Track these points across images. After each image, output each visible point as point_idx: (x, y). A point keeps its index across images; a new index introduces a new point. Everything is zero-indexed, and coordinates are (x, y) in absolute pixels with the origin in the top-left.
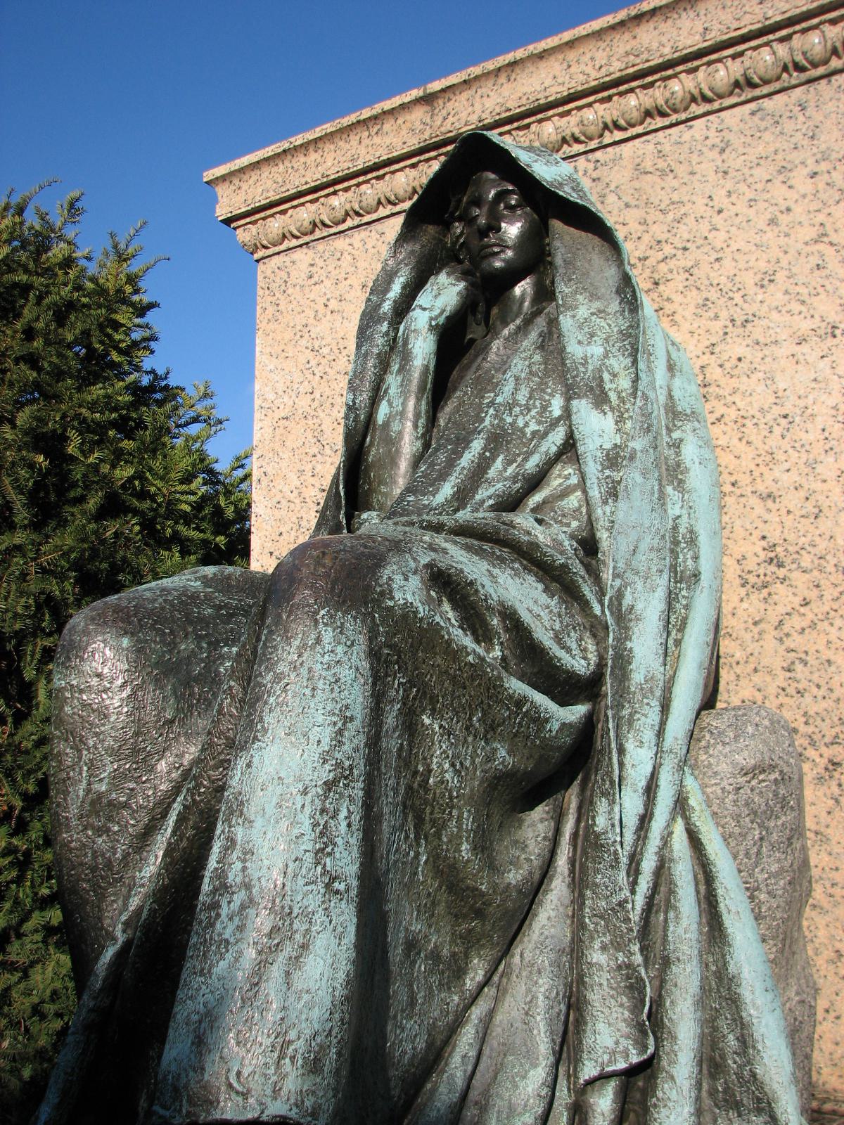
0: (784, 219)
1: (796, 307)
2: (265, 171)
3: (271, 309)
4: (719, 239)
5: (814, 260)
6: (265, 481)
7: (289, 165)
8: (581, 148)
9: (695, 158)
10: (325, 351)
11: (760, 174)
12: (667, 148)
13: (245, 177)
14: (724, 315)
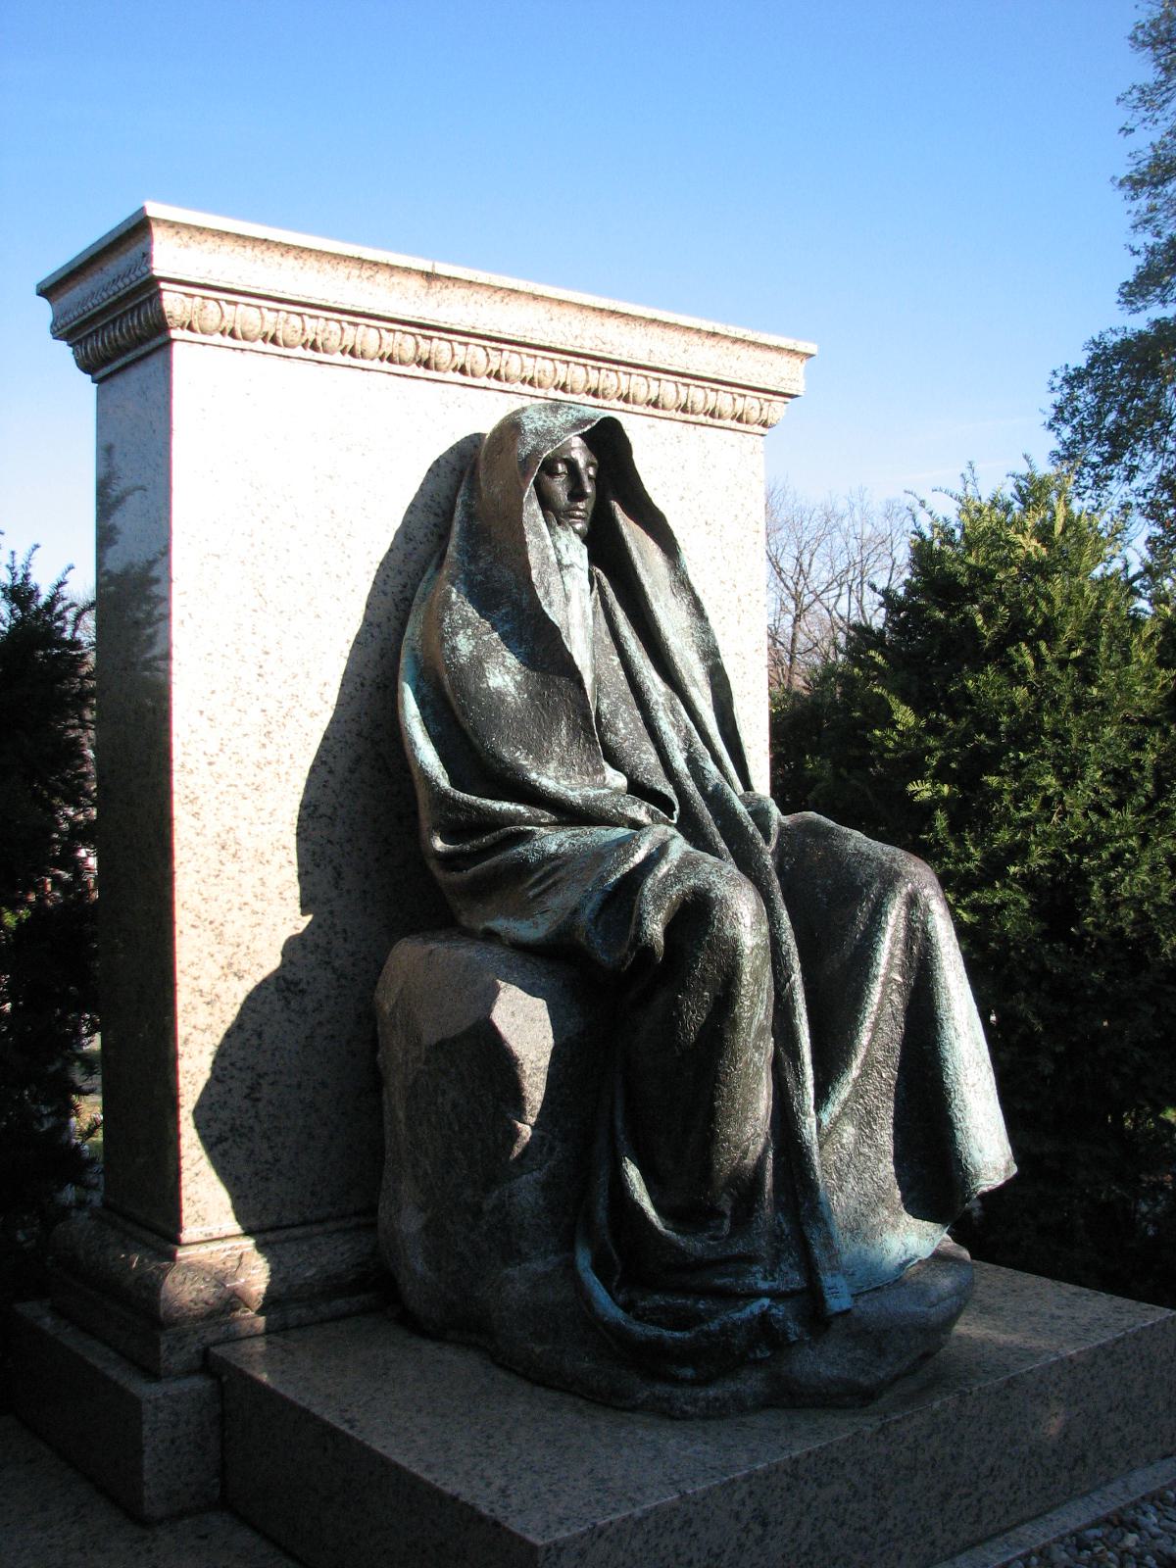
7: (259, 255)
13: (199, 237)
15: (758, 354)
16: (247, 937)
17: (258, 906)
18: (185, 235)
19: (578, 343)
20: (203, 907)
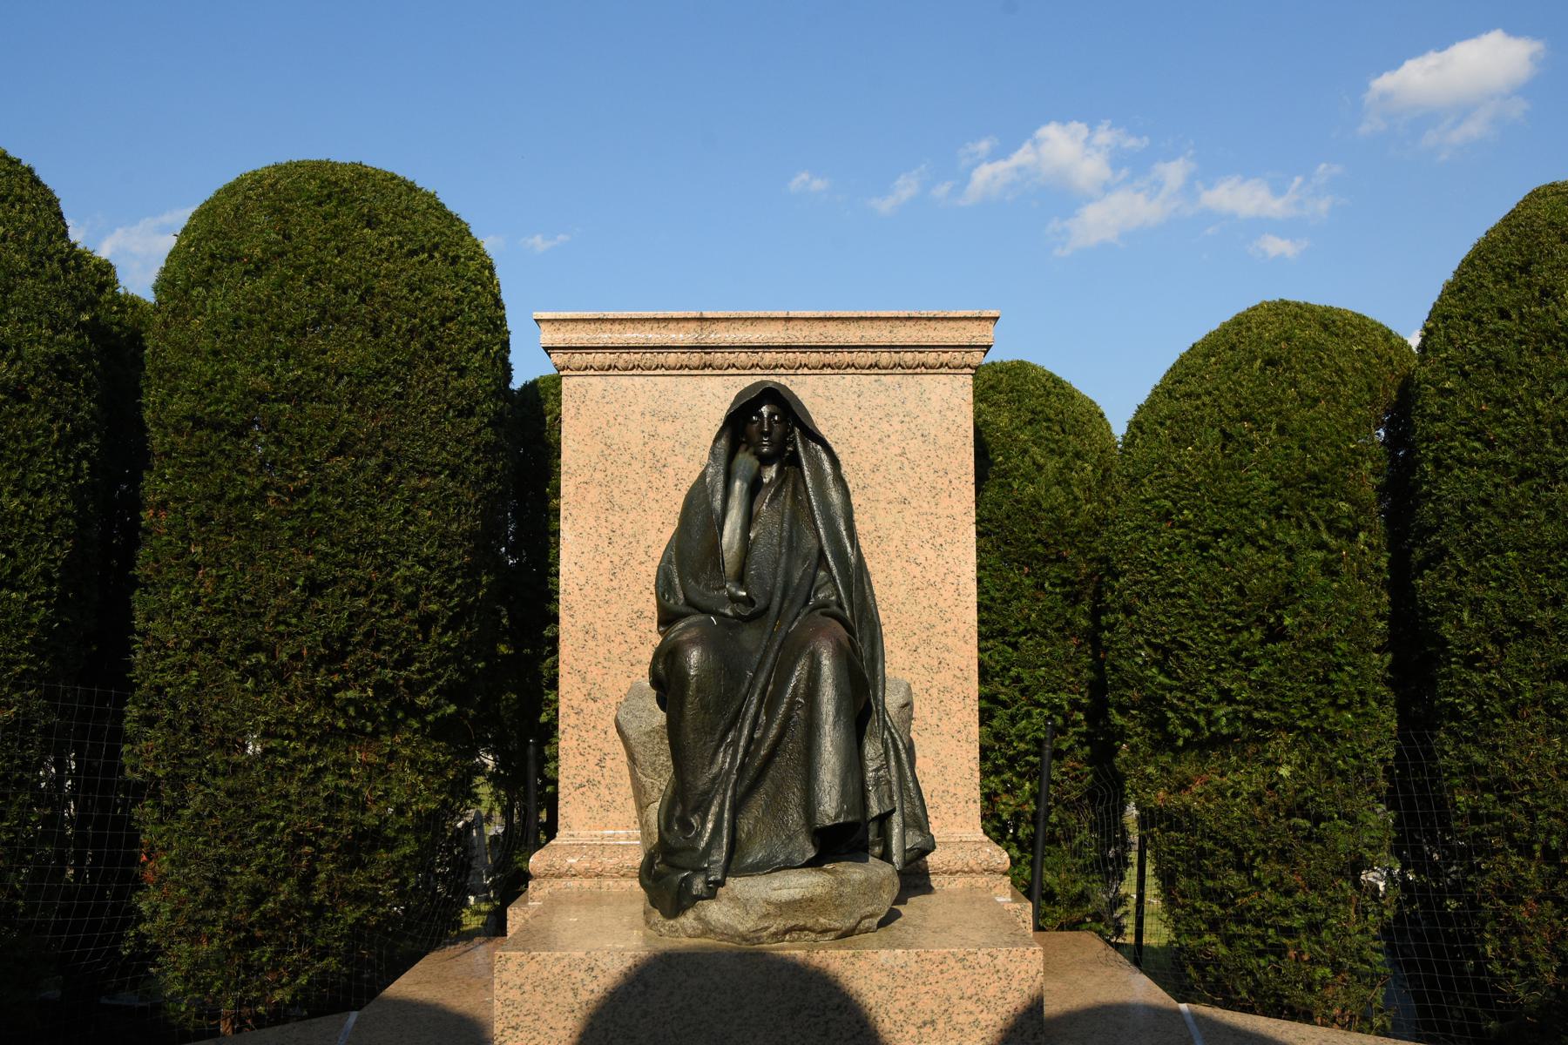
2: (580, 326)
3: (573, 411)
4: (854, 442)
6: (570, 519)
15: (951, 324)
16: (599, 680)
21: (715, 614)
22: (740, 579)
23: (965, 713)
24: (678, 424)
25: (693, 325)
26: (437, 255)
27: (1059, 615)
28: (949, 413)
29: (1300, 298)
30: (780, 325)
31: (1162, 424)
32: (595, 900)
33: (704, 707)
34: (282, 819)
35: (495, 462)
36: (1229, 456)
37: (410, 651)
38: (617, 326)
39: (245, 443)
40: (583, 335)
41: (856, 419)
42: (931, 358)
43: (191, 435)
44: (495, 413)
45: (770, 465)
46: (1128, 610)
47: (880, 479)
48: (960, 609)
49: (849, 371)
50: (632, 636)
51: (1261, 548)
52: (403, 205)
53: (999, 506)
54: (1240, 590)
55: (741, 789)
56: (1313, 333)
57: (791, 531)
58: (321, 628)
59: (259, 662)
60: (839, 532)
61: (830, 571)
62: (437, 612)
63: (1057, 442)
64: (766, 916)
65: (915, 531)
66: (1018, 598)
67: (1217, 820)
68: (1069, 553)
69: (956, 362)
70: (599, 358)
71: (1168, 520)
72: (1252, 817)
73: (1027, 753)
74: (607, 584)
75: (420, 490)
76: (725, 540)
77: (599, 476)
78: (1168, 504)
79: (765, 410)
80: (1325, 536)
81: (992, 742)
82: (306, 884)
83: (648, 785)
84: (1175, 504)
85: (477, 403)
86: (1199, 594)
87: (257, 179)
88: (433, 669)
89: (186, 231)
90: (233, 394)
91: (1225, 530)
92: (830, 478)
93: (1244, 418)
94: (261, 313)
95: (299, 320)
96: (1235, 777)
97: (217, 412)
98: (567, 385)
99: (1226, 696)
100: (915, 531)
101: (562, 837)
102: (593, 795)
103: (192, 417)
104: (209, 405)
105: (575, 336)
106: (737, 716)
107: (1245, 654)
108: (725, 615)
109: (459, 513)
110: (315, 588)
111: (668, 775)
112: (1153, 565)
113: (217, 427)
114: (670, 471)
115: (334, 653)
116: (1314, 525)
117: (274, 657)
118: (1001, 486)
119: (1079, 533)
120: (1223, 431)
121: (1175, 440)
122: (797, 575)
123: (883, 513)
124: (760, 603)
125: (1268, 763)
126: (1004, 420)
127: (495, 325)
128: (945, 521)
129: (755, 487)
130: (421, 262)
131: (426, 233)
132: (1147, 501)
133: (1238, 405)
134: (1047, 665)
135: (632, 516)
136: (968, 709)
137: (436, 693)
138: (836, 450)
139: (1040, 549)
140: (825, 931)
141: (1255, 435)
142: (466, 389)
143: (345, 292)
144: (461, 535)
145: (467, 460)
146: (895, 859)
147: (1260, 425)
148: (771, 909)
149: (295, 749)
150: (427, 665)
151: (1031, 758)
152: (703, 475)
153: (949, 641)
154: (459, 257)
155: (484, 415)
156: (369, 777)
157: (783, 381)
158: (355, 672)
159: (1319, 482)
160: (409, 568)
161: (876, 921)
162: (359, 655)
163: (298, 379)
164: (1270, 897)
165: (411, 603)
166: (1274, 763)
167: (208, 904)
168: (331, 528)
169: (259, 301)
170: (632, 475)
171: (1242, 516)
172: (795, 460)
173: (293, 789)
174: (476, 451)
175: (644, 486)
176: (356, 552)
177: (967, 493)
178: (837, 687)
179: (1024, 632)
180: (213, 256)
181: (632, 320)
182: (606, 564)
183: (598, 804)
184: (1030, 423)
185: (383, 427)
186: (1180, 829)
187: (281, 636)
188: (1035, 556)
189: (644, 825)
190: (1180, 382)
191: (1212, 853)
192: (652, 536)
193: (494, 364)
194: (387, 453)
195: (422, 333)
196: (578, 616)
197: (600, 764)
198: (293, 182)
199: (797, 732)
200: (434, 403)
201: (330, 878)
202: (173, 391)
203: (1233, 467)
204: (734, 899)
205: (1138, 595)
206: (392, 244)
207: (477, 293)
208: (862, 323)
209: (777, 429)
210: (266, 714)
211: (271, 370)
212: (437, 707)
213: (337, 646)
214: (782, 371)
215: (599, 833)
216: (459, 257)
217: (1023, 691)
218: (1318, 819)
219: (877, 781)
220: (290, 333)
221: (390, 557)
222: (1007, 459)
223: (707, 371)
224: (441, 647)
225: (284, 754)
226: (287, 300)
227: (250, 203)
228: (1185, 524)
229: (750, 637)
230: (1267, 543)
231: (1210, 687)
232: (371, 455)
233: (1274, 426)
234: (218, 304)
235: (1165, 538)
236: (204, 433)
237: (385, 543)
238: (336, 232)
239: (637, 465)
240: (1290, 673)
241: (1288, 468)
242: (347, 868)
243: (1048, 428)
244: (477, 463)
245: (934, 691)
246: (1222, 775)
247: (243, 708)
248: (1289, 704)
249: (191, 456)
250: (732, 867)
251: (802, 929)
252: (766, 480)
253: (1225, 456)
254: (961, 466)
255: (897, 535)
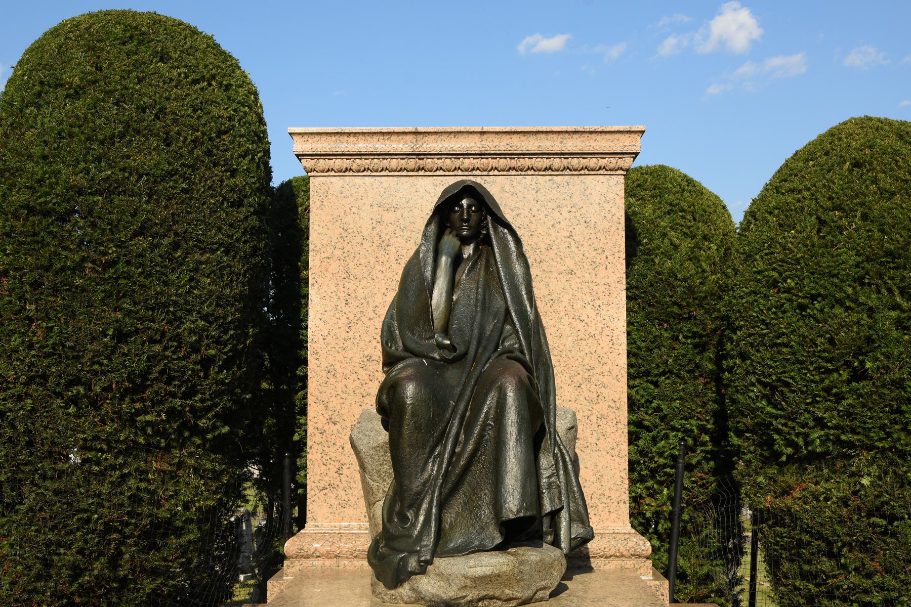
0: (558, 226)
1: (559, 260)
2: (324, 138)
3: (318, 203)
4: (533, 227)
5: (567, 244)
6: (316, 285)
8: (480, 173)
9: (526, 191)
10: (350, 231)
11: (551, 205)
12: (515, 184)
14: (532, 257)
15: (608, 136)
16: (338, 407)
17: (343, 396)
18: (306, 137)
19: (497, 148)
20: (319, 395)
21: (427, 357)
22: (446, 331)
23: (618, 435)
24: (398, 213)
25: (410, 138)
26: (214, 83)
27: (690, 360)
28: (605, 205)
29: (882, 116)
30: (476, 138)
31: (771, 213)
32: (334, 576)
33: (418, 428)
34: (96, 512)
35: (259, 242)
36: (823, 237)
37: (195, 385)
38: (351, 139)
39: (68, 226)
40: (326, 145)
41: (534, 209)
42: (592, 162)
43: (27, 219)
44: (259, 204)
45: (469, 244)
46: (744, 356)
47: (553, 256)
48: (614, 355)
49: (529, 172)
50: (363, 374)
51: (848, 309)
52: (188, 45)
53: (645, 277)
54: (831, 341)
55: (445, 491)
56: (891, 141)
57: (484, 295)
58: (126, 367)
59: (79, 392)
60: (521, 295)
61: (514, 325)
62: (215, 356)
63: (690, 227)
64: (464, 587)
65: (580, 295)
66: (658, 347)
67: (813, 518)
68: (699, 313)
69: (612, 166)
70: (338, 163)
71: (775, 287)
72: (840, 516)
73: (665, 466)
74: (344, 335)
75: (202, 263)
76: (434, 302)
77: (338, 253)
78: (776, 275)
79: (465, 202)
80: (898, 299)
81: (638, 457)
82: (114, 563)
83: (375, 488)
84: (780, 274)
85: (245, 196)
86: (799, 344)
87: (75, 24)
88: (211, 399)
89: (20, 64)
90: (58, 189)
91: (819, 295)
92: (514, 254)
93: (835, 208)
94: (80, 126)
95: (108, 133)
96: (827, 486)
97: (46, 202)
98: (314, 183)
99: (820, 423)
100: (580, 295)
101: (309, 527)
102: (333, 496)
103: (27, 207)
104: (40, 197)
105: (320, 145)
106: (443, 435)
107: (835, 390)
108: (434, 359)
109: (232, 281)
110: (121, 336)
111: (390, 480)
112: (763, 322)
113: (46, 214)
114: (392, 249)
115: (137, 386)
116: (890, 291)
117: (90, 390)
118: (646, 261)
119: (706, 297)
120: (818, 218)
121: (781, 225)
122: (489, 328)
123: (555, 281)
124: (460, 349)
125: (853, 475)
126: (648, 211)
127: (259, 137)
128: (602, 288)
129: (457, 261)
130: (202, 89)
131: (206, 66)
132: (759, 272)
133: (830, 198)
134: (681, 398)
135: (362, 284)
136: (620, 432)
137: (214, 417)
138: (519, 233)
139: (675, 309)
140: (509, 600)
141: (844, 222)
142: (237, 186)
143: (144, 111)
144: (234, 297)
145: (238, 240)
146: (563, 545)
147: (848, 214)
148: (468, 582)
149: (106, 459)
150: (207, 396)
151: (668, 470)
152: (417, 252)
153: (606, 380)
154: (231, 85)
155: (250, 206)
156: (163, 482)
157: (478, 180)
158: (152, 401)
159: (894, 258)
160: (193, 322)
161: (548, 592)
162: (155, 388)
163: (108, 178)
164: (854, 579)
165: (195, 348)
166: (858, 474)
167: (39, 577)
168: (134, 291)
169: (78, 118)
170: (363, 252)
171: (832, 283)
172: (487, 241)
173: (105, 489)
174: (244, 233)
175: (373, 261)
176: (153, 309)
177: (619, 265)
178: (519, 412)
179: (663, 373)
180: (42, 83)
181: (363, 134)
182: (344, 319)
183: (337, 502)
184: (669, 213)
185: (173, 214)
186: (783, 525)
187: (96, 373)
188: (672, 315)
189: (371, 518)
190: (785, 181)
191: (809, 544)
192: (378, 299)
193: (258, 167)
194: (176, 234)
195: (203, 144)
196: (322, 359)
197: (339, 472)
198: (103, 27)
199: (489, 447)
200: (212, 196)
201: (132, 558)
202: (11, 187)
203: (826, 246)
204: (440, 575)
205: (752, 345)
206: (179, 74)
207: (245, 113)
208: (539, 136)
209: (474, 217)
210: (84, 432)
211: (87, 171)
212: (215, 427)
213: (138, 381)
214: (478, 172)
215: (337, 524)
216: (231, 85)
217: (662, 419)
218: (892, 519)
219: (550, 486)
220: (102, 143)
221: (179, 314)
222: (651, 240)
223: (421, 173)
224: (217, 383)
225: (98, 463)
226: (99, 118)
227: (70, 42)
228: (788, 290)
229: (453, 375)
230: (852, 305)
231: (807, 416)
232: (164, 236)
233: (859, 214)
234: (46, 120)
235: (773, 300)
236: (36, 219)
237: (175, 303)
238: (137, 65)
239: (367, 245)
240: (870, 405)
241: (870, 247)
242: (147, 550)
243: (683, 217)
244: (245, 242)
245: (593, 418)
246: (817, 483)
247: (67, 428)
248: (870, 429)
249: (26, 236)
250: (438, 550)
251: (492, 598)
252: (465, 256)
253: (820, 237)
254: (615, 246)
255: (566, 298)
